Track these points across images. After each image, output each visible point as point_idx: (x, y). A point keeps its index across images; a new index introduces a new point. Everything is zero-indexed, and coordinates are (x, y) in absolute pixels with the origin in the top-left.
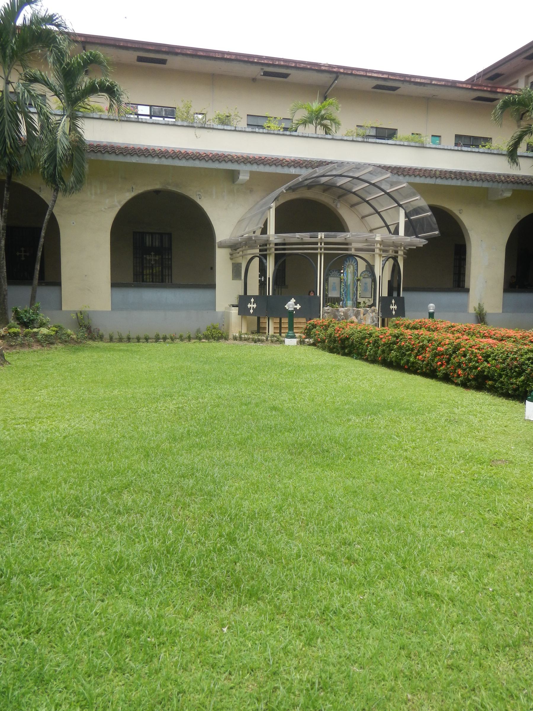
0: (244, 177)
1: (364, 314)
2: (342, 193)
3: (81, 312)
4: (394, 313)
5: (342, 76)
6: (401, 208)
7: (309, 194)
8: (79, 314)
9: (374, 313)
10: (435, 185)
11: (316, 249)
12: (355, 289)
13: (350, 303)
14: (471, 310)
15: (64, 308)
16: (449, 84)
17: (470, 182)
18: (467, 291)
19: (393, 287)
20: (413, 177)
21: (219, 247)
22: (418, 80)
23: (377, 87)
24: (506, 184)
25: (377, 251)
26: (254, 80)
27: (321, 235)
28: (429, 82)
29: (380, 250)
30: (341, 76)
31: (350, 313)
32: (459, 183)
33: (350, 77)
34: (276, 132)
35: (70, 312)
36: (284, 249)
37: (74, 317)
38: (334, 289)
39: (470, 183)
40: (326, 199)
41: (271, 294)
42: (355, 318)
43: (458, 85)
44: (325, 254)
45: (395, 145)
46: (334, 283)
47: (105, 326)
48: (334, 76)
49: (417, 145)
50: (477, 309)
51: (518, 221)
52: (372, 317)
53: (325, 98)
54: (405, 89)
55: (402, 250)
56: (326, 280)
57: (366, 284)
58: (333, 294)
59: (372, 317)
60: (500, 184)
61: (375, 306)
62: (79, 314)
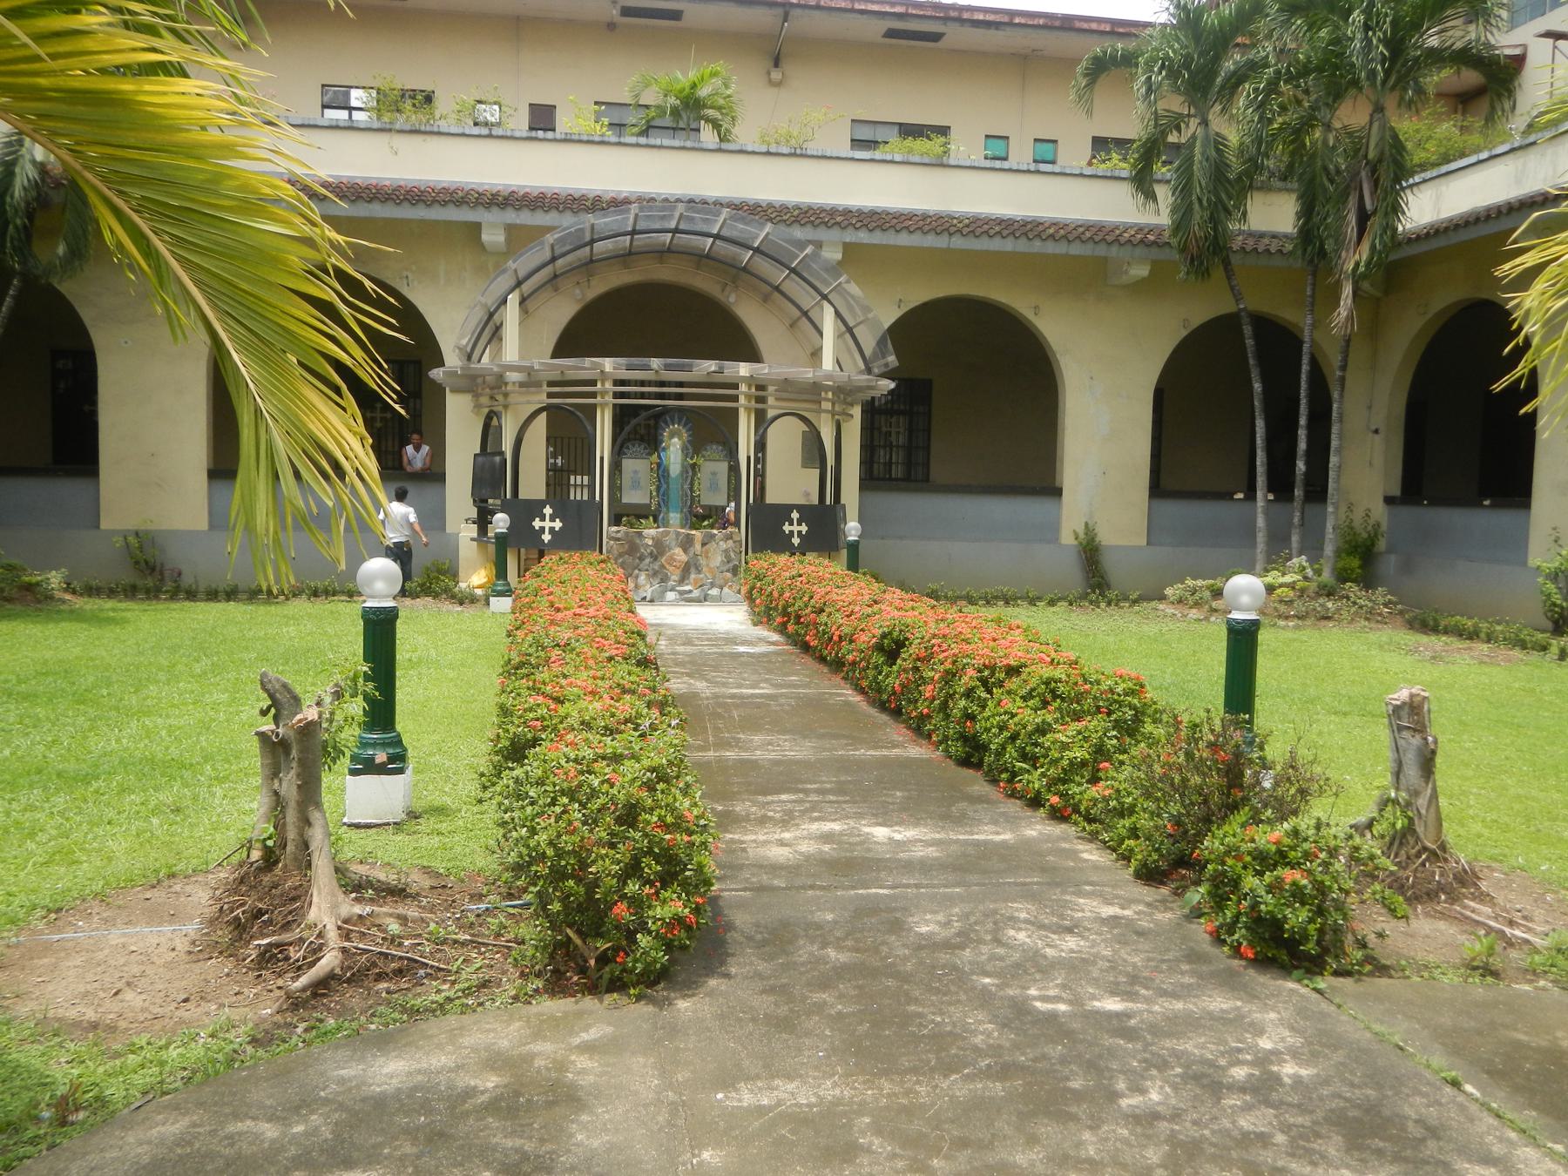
0: (493, 236)
1: (704, 544)
2: (738, 274)
3: (137, 534)
5: (798, 11)
6: (825, 303)
7: (665, 273)
8: (131, 539)
10: (948, 251)
11: (593, 395)
13: (675, 517)
14: (1067, 538)
15: (103, 527)
16: (1057, 24)
17: (1037, 243)
18: (1057, 492)
20: (892, 231)
21: (453, 391)
22: (981, 17)
23: (891, 34)
24: (1129, 248)
25: (742, 400)
26: (611, 26)
27: (608, 364)
28: (1006, 19)
29: (749, 397)
30: (795, 12)
31: (670, 540)
32: (1008, 245)
33: (817, 13)
34: (585, 138)
35: (114, 532)
36: (680, 397)
37: (119, 542)
38: (636, 485)
39: (1037, 246)
40: (704, 282)
43: (1078, 24)
44: (615, 405)
45: (872, 160)
46: (636, 472)
47: (194, 565)
48: (780, 11)
49: (926, 160)
50: (1082, 536)
51: (1184, 333)
53: (776, 63)
54: (956, 36)
55: (827, 400)
56: (616, 467)
57: (714, 474)
58: (632, 497)
59: (726, 551)
60: (1114, 249)
62: (131, 539)
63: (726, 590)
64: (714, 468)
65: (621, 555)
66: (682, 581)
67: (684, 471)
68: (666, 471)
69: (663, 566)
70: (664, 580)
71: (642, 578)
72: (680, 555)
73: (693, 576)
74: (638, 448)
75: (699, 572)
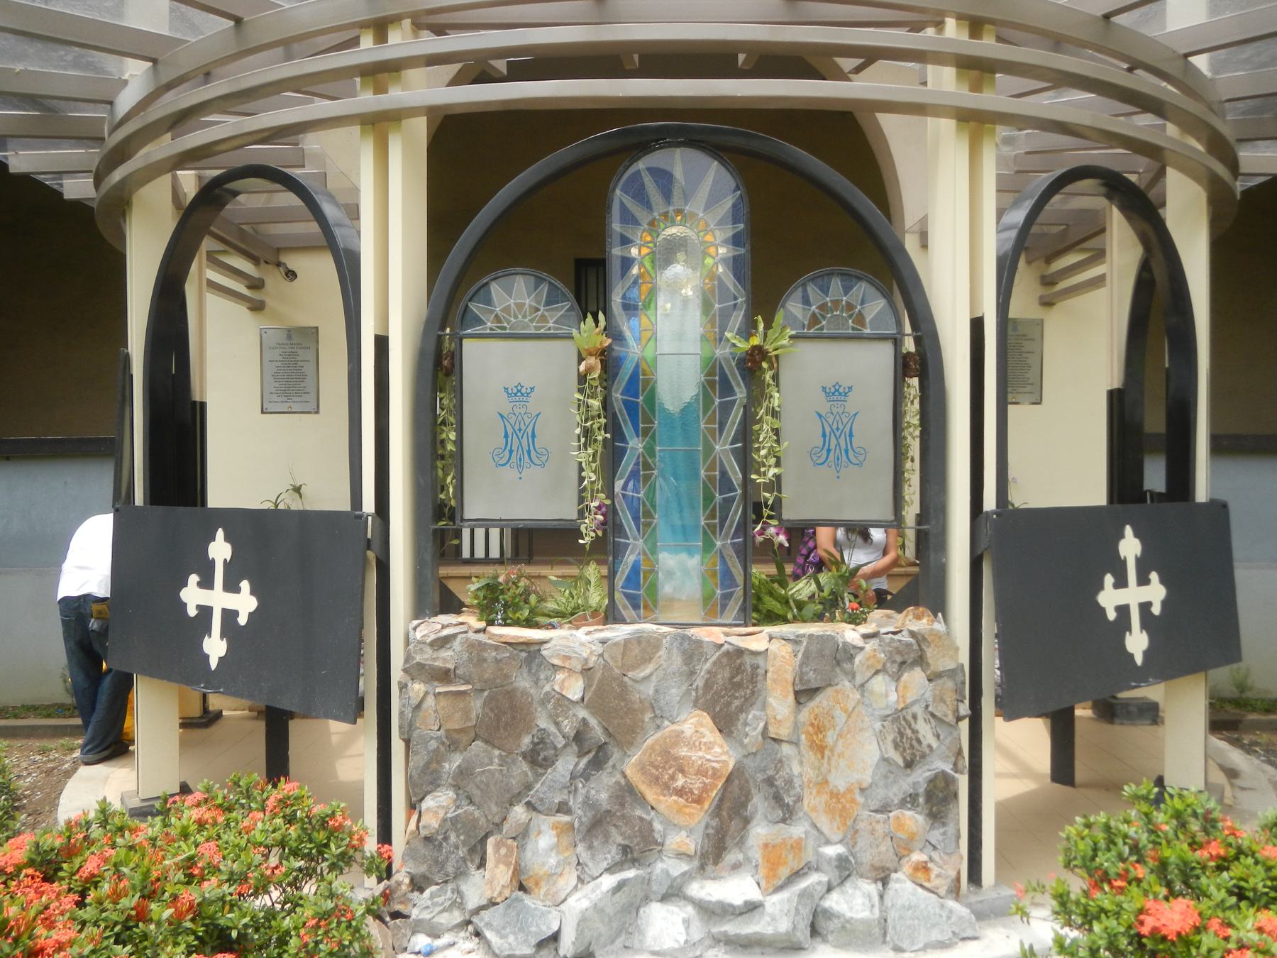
1: (804, 694)
4: (1137, 643)
9: (915, 677)
12: (635, 444)
13: (681, 569)
19: (1143, 431)
31: (657, 679)
38: (520, 445)
41: (139, 499)
42: (710, 733)
46: (518, 393)
52: (900, 720)
56: (440, 369)
57: (836, 393)
59: (900, 720)
61: (938, 605)
63: (903, 886)
64: (832, 372)
65: (453, 743)
66: (715, 852)
67: (716, 381)
68: (641, 384)
69: (627, 793)
70: (640, 849)
71: (545, 844)
72: (702, 744)
73: (760, 831)
74: (514, 295)
75: (787, 813)
